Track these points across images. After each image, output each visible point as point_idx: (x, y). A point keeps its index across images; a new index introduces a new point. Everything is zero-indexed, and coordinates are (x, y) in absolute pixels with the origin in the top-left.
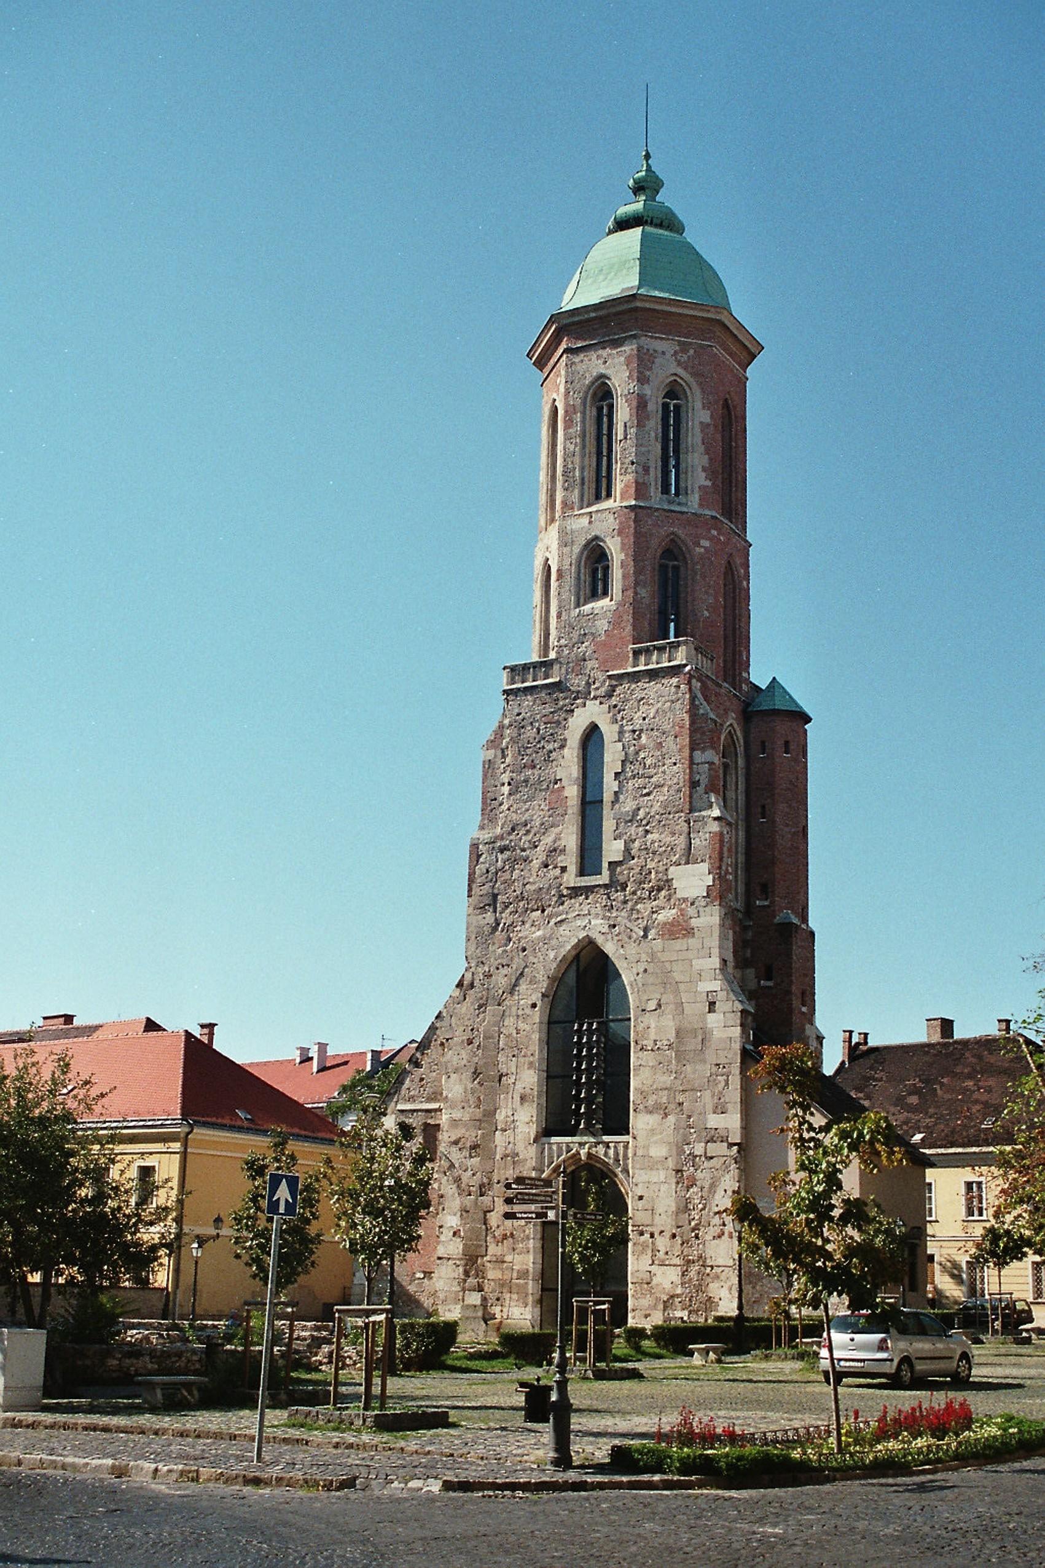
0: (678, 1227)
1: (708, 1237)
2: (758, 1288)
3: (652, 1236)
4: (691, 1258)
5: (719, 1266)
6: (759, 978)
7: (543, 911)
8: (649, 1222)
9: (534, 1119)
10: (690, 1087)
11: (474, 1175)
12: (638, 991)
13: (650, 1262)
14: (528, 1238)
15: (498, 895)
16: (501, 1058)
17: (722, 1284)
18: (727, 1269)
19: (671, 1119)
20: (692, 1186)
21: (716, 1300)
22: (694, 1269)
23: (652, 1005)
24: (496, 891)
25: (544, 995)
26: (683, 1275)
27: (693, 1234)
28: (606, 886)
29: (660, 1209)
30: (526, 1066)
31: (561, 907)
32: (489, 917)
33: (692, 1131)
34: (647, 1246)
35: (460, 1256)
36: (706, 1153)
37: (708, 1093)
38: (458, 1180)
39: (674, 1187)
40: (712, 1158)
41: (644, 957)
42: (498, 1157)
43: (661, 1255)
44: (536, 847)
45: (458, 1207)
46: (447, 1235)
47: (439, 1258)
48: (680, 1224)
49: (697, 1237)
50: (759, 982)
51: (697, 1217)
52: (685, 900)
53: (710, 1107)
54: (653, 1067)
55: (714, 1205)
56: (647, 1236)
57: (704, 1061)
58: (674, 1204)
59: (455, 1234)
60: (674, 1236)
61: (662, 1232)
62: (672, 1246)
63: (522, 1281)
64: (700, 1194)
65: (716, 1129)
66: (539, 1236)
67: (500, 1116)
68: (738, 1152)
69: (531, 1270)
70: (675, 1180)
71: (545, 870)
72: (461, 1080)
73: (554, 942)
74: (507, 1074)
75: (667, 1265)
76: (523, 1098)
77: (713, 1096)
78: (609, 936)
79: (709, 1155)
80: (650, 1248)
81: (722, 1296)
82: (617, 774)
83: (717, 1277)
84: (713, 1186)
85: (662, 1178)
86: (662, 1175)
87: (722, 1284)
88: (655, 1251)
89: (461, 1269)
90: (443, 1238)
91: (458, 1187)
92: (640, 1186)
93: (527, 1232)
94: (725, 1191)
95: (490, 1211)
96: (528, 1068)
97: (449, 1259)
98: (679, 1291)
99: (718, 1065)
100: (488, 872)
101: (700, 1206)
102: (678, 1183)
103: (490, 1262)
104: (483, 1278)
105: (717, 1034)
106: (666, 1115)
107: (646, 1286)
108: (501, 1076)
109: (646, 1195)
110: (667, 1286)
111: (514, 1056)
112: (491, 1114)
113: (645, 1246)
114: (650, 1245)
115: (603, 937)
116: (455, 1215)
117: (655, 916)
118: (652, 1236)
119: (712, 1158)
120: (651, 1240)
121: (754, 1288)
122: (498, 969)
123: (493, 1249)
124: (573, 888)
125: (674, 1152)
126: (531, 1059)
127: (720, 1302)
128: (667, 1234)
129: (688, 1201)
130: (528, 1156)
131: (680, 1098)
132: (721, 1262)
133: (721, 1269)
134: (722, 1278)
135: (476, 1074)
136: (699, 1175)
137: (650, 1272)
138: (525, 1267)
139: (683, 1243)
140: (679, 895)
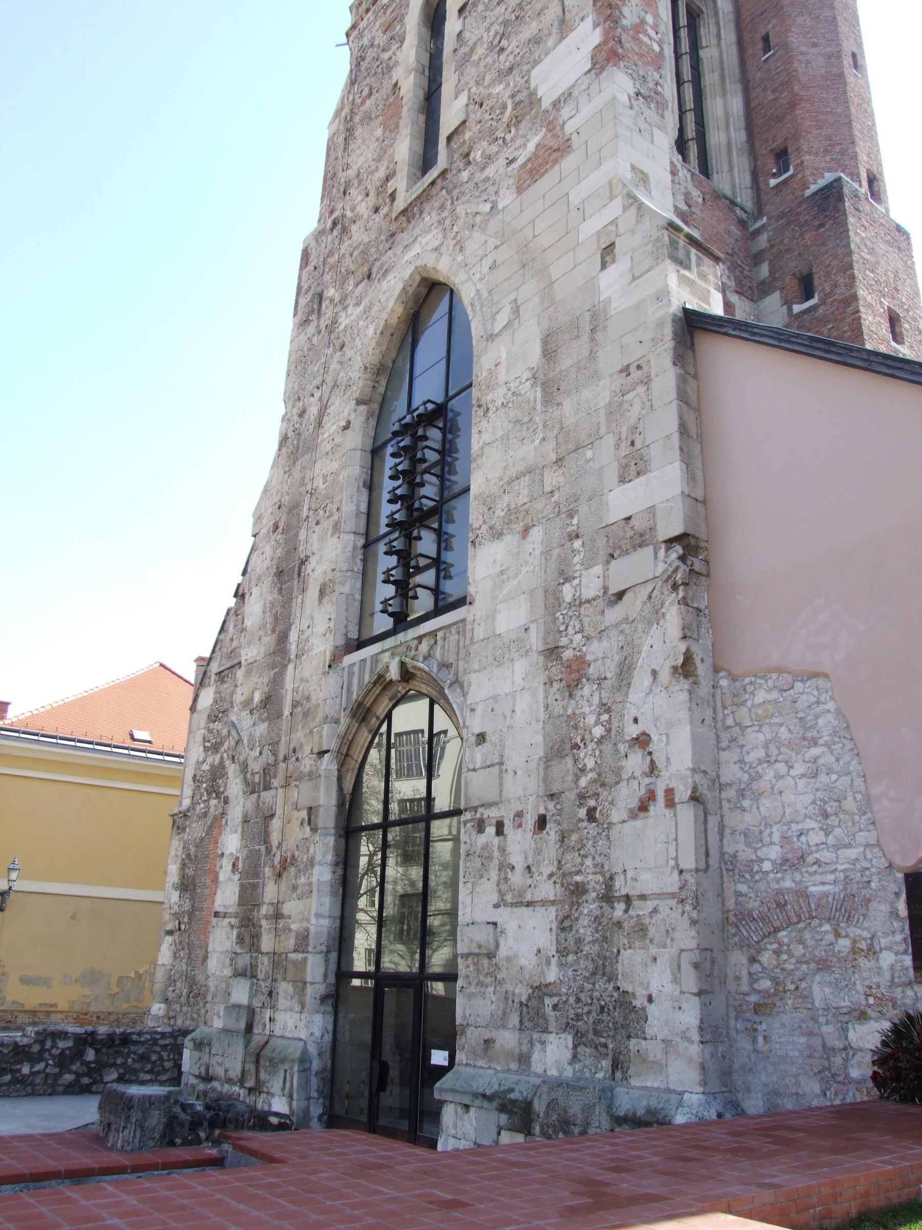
0: (552, 796)
1: (616, 816)
2: (766, 958)
3: (500, 829)
4: (578, 878)
5: (643, 897)
6: (788, 303)
7: (369, 276)
8: (494, 797)
9: (332, 624)
10: (571, 446)
11: (261, 753)
12: (481, 309)
13: (495, 898)
14: (311, 863)
15: (323, 292)
16: (302, 536)
17: (654, 951)
18: (664, 906)
19: (536, 534)
20: (578, 681)
21: (637, 1003)
22: (590, 906)
23: (502, 320)
24: (319, 290)
25: (359, 402)
26: (563, 929)
27: (582, 812)
28: (443, 174)
29: (514, 760)
30: (330, 532)
31: (390, 253)
32: (311, 329)
33: (577, 544)
34: (490, 858)
35: (232, 910)
36: (605, 589)
37: (610, 440)
38: (244, 767)
39: (541, 694)
40: (620, 595)
41: (492, 242)
42: (286, 712)
43: (517, 878)
44: (367, 195)
45: (240, 819)
46: (225, 870)
47: (216, 914)
48: (555, 788)
49: (591, 815)
50: (790, 309)
51: (590, 763)
52: (556, 104)
53: (612, 472)
54: (502, 438)
55: (628, 719)
56: (491, 830)
57: (596, 376)
58: (539, 739)
59: (234, 865)
60: (542, 822)
61: (519, 815)
62: (538, 852)
63: (298, 956)
64: (596, 700)
65: (629, 518)
66: (330, 857)
67: (293, 637)
68: (682, 558)
69: (312, 929)
70: (542, 678)
71: (374, 216)
72: (261, 595)
73: (375, 309)
74: (307, 557)
75: (529, 904)
76: (322, 593)
77: (617, 446)
78: (443, 249)
79: (613, 590)
80: (496, 862)
81: (654, 990)
82: (461, 11)
83: (642, 930)
84: (625, 670)
85: (519, 680)
86: (520, 667)
87: (654, 951)
88: (506, 867)
89: (235, 932)
90: (222, 877)
91: (245, 779)
92: (480, 709)
93: (312, 850)
94: (654, 673)
95: (273, 816)
96: (332, 535)
97: (225, 915)
98: (552, 974)
99: (626, 370)
100: (315, 268)
101: (598, 731)
102: (550, 682)
103: (267, 917)
104: (257, 951)
105: (618, 305)
106: (526, 531)
107: (485, 962)
108: (303, 563)
109: (489, 729)
110: (527, 960)
111: (317, 523)
112: (283, 638)
113: (485, 857)
114: (496, 854)
115: (435, 255)
116: (236, 832)
117: (510, 169)
118: (500, 829)
119: (620, 595)
120: (496, 841)
121: (753, 960)
122: (313, 395)
123: (270, 891)
124: (404, 212)
125: (541, 611)
126: (336, 517)
127: (652, 1010)
128: (530, 821)
129: (573, 721)
130: (322, 695)
131: (552, 479)
132: (648, 882)
133: (650, 905)
134: (652, 931)
135: (280, 573)
136: (594, 650)
137: (495, 924)
138: (305, 925)
139: (562, 840)
140: (546, 104)
